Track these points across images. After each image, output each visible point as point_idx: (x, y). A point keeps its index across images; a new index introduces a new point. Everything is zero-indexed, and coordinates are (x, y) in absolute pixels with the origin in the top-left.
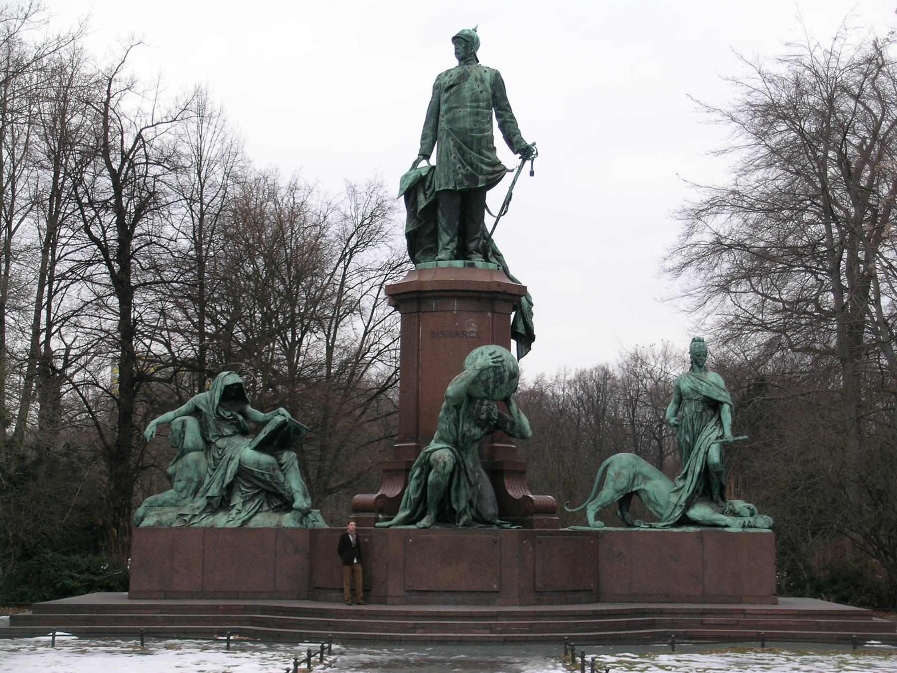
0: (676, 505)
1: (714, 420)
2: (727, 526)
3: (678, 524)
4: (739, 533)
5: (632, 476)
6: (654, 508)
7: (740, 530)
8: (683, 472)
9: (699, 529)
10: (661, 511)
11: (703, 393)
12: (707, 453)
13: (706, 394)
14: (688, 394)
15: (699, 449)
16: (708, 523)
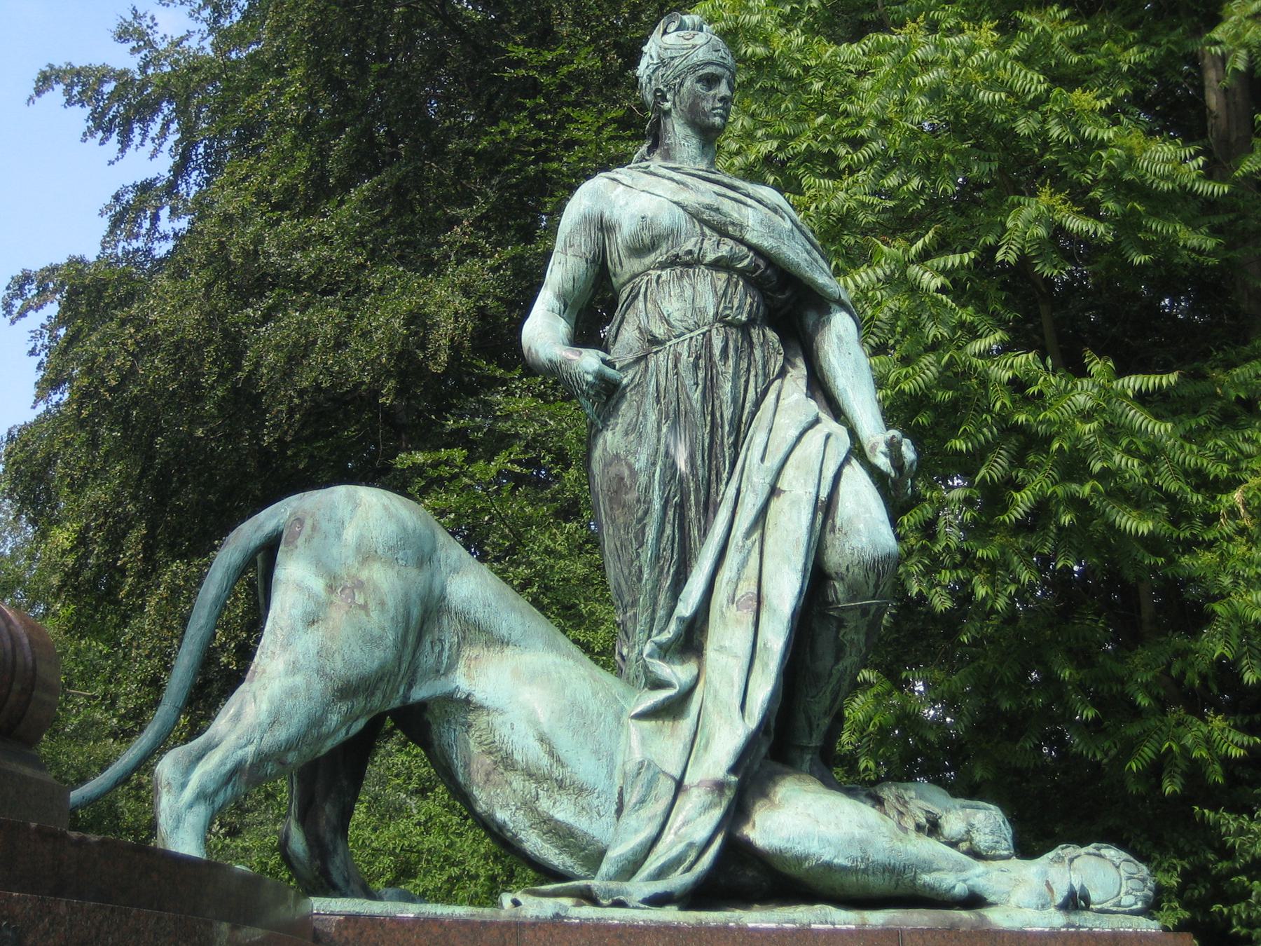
0: (679, 786)
1: (798, 374)
2: (974, 901)
3: (697, 897)
4: (1053, 935)
5: (416, 612)
6: (529, 806)
7: (1057, 920)
8: (687, 606)
9: (876, 918)
10: (582, 824)
11: (751, 237)
12: (826, 508)
13: (767, 243)
14: (672, 234)
15: (774, 491)
16: (879, 884)
